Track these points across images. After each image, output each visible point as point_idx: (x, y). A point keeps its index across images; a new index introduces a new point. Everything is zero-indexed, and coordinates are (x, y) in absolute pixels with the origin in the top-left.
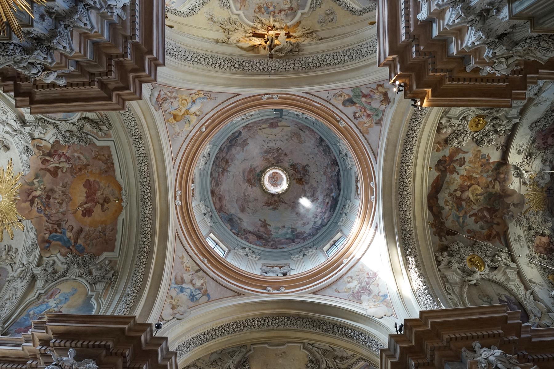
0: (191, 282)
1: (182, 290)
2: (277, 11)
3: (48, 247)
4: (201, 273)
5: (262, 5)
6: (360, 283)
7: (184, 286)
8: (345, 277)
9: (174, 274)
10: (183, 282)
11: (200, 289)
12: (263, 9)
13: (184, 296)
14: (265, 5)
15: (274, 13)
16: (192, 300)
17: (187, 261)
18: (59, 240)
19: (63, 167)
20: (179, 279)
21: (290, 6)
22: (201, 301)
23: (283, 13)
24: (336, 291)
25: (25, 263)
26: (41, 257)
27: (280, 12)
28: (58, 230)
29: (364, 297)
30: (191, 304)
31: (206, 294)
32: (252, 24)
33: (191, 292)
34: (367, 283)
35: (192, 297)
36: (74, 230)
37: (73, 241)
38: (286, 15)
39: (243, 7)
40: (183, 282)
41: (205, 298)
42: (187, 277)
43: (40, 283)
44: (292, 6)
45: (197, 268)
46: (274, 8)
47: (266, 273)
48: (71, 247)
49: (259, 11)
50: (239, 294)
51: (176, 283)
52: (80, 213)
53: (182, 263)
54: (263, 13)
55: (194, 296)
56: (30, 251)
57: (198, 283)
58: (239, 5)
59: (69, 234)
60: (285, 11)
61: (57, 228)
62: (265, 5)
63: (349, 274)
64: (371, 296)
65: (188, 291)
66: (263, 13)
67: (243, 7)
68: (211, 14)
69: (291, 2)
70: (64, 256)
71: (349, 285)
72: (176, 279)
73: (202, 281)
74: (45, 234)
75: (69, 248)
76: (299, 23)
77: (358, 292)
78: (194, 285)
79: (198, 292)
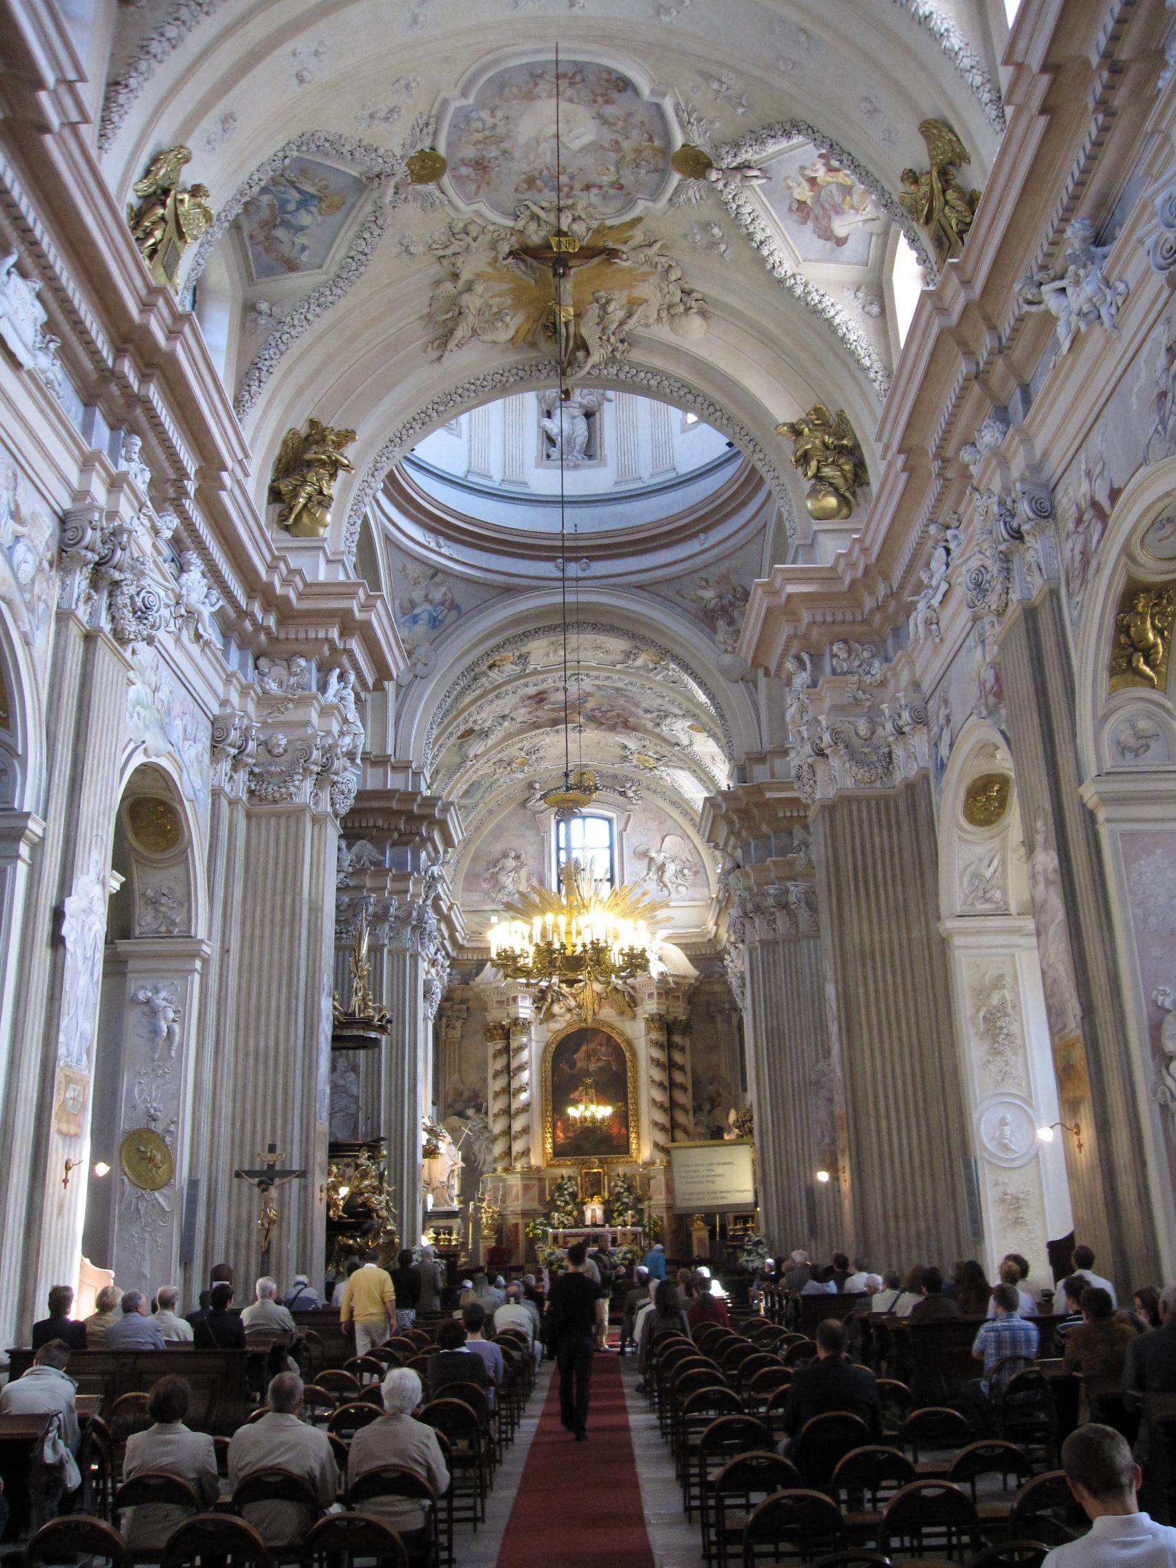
0: (427, 599)
1: (415, 620)
2: (577, 186)
4: (439, 578)
5: (536, 174)
6: (720, 597)
7: (417, 611)
8: (696, 576)
9: (397, 602)
10: (413, 605)
11: (442, 603)
12: (539, 183)
13: (421, 628)
14: (545, 173)
15: (571, 188)
16: (434, 627)
17: (413, 570)
20: (407, 604)
21: (613, 178)
22: (447, 622)
23: (595, 191)
24: (678, 592)
27: (587, 188)
29: (721, 624)
30: (435, 633)
31: (454, 606)
32: (510, 223)
33: (430, 615)
34: (732, 604)
35: (434, 622)
38: (604, 197)
39: (484, 186)
40: (413, 605)
41: (454, 613)
42: (418, 595)
44: (622, 181)
45: (431, 572)
46: (572, 178)
47: (549, 415)
49: (529, 188)
50: (507, 591)
51: (404, 614)
53: (406, 577)
54: (540, 191)
55: (435, 619)
57: (437, 595)
58: (473, 187)
60: (600, 187)
62: (545, 173)
63: (703, 574)
64: (731, 629)
65: (425, 616)
66: (540, 191)
67: (484, 186)
68: (405, 242)
69: (618, 171)
71: (701, 593)
72: (401, 606)
73: (443, 589)
76: (637, 221)
77: (713, 611)
78: (431, 602)
79: (440, 608)
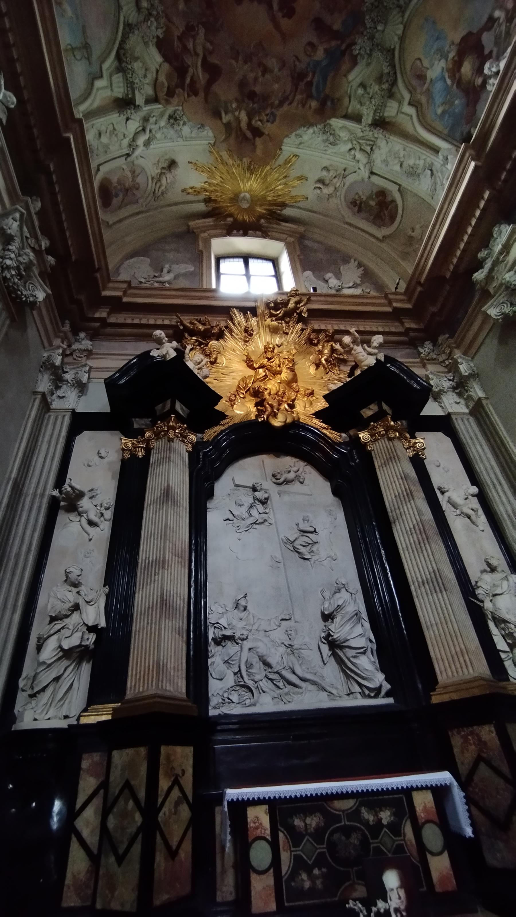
3: (332, 101)
18: (325, 78)
19: (204, 47)
25: (350, 146)
26: (346, 117)
28: (309, 79)
36: (315, 41)
37: (334, 43)
43: (391, 110)
48: (343, 47)
52: (285, 23)
56: (331, 138)
59: (320, 54)
61: (305, 81)
70: (354, 63)
74: (310, 107)
75: (343, 53)
